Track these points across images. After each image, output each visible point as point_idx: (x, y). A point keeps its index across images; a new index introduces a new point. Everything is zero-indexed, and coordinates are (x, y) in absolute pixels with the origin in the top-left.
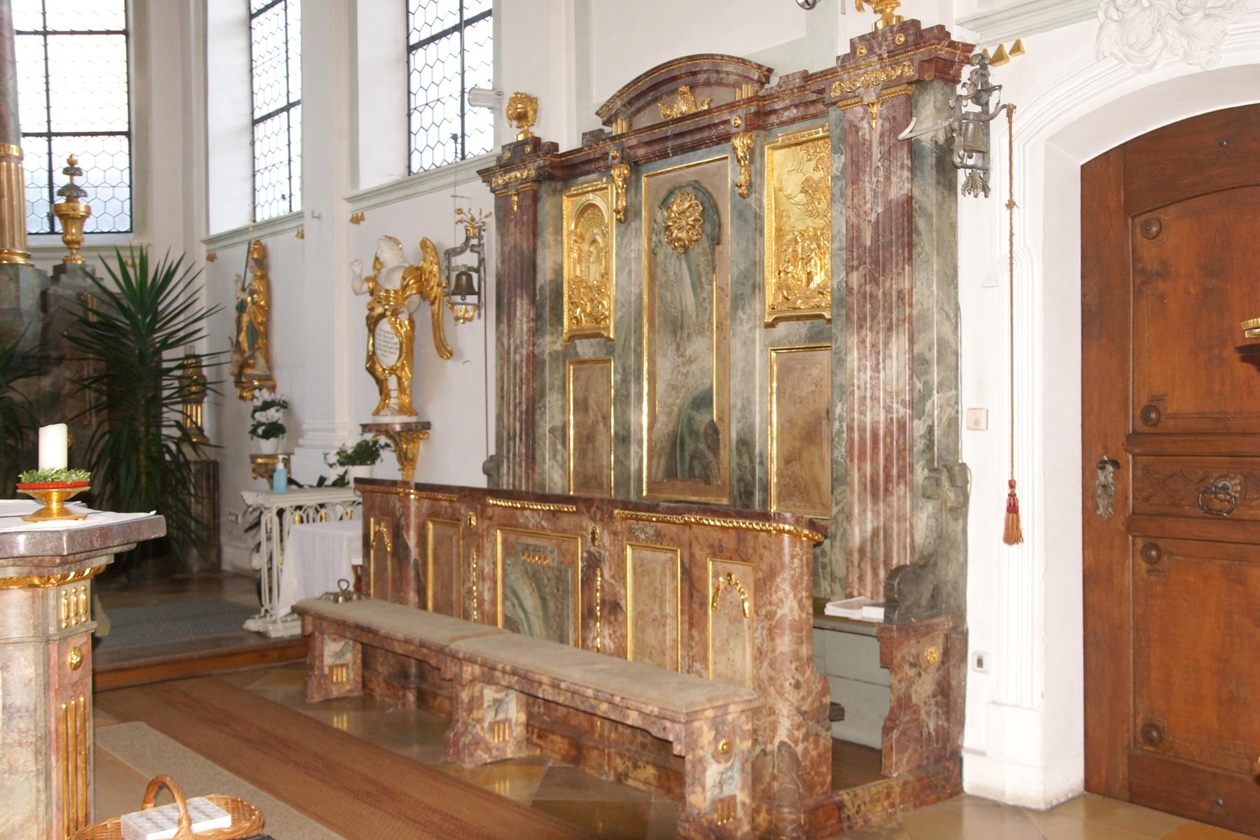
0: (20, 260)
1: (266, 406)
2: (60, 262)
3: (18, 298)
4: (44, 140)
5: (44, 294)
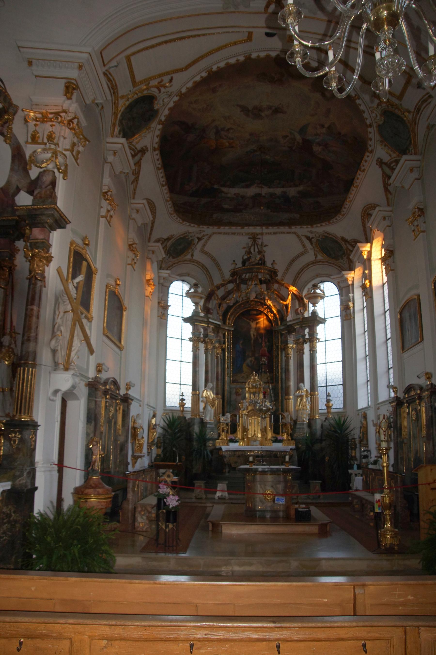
0: (317, 417)
1: (364, 451)
2: (326, 417)
3: (316, 426)
4: (325, 388)
5: (322, 425)
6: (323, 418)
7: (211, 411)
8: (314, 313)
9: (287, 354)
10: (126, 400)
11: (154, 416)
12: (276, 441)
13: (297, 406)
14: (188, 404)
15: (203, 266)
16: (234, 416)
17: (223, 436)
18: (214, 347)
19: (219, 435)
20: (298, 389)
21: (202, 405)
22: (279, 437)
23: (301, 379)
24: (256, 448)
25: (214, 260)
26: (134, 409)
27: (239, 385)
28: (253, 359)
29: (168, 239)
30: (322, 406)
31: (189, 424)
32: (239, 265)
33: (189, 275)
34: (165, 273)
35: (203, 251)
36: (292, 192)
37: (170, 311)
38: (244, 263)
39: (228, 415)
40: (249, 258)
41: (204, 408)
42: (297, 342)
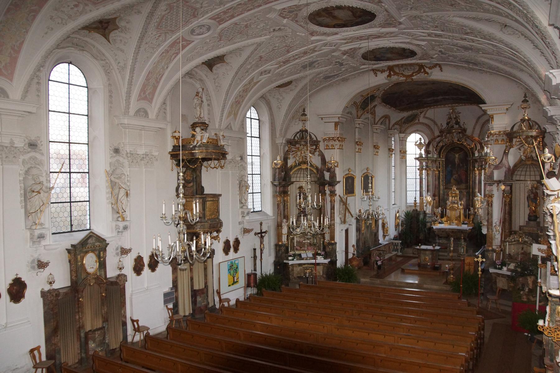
11: (398, 212)
12: (463, 224)
15: (426, 124)
21: (425, 204)
25: (432, 120)
28: (457, 176)
32: (445, 125)
34: (402, 135)
35: (424, 117)
36: (463, 97)
37: (407, 153)
38: (448, 124)
39: (440, 208)
40: (449, 122)
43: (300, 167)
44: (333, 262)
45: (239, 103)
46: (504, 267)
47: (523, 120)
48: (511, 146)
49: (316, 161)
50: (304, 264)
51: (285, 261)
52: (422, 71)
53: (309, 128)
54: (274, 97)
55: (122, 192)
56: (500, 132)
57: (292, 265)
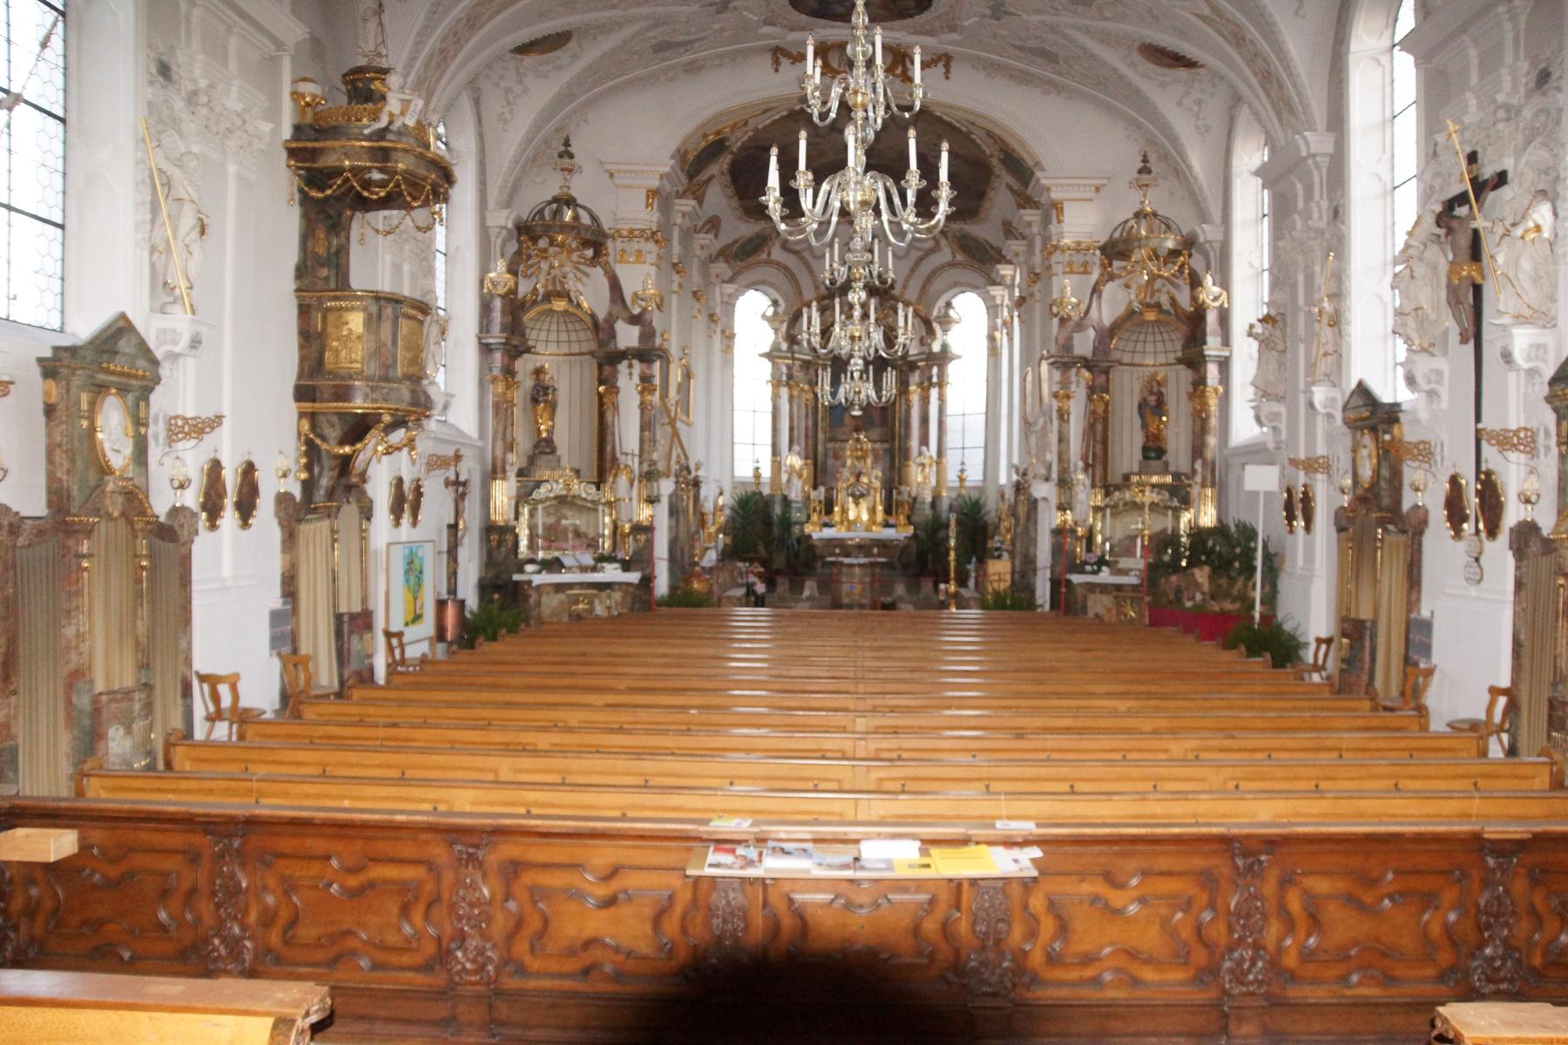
6: (954, 495)
7: (797, 484)
8: (945, 347)
9: (908, 401)
10: (696, 484)
12: (887, 525)
13: (920, 479)
14: (766, 473)
16: (830, 490)
17: (815, 517)
18: (802, 390)
19: (809, 517)
20: (920, 454)
21: (784, 477)
22: (892, 521)
23: (924, 441)
24: (857, 535)
26: (703, 492)
27: (837, 445)
29: (735, 242)
30: (952, 476)
31: (767, 503)
33: (764, 283)
37: (736, 339)
41: (789, 481)
42: (920, 385)
43: (547, 306)
44: (647, 581)
45: (445, 59)
46: (1104, 568)
47: (1139, 215)
48: (1112, 277)
49: (592, 295)
50: (570, 586)
51: (516, 577)
52: (899, 71)
53: (579, 188)
54: (497, 85)
55: (188, 221)
56: (1079, 244)
57: (539, 587)
